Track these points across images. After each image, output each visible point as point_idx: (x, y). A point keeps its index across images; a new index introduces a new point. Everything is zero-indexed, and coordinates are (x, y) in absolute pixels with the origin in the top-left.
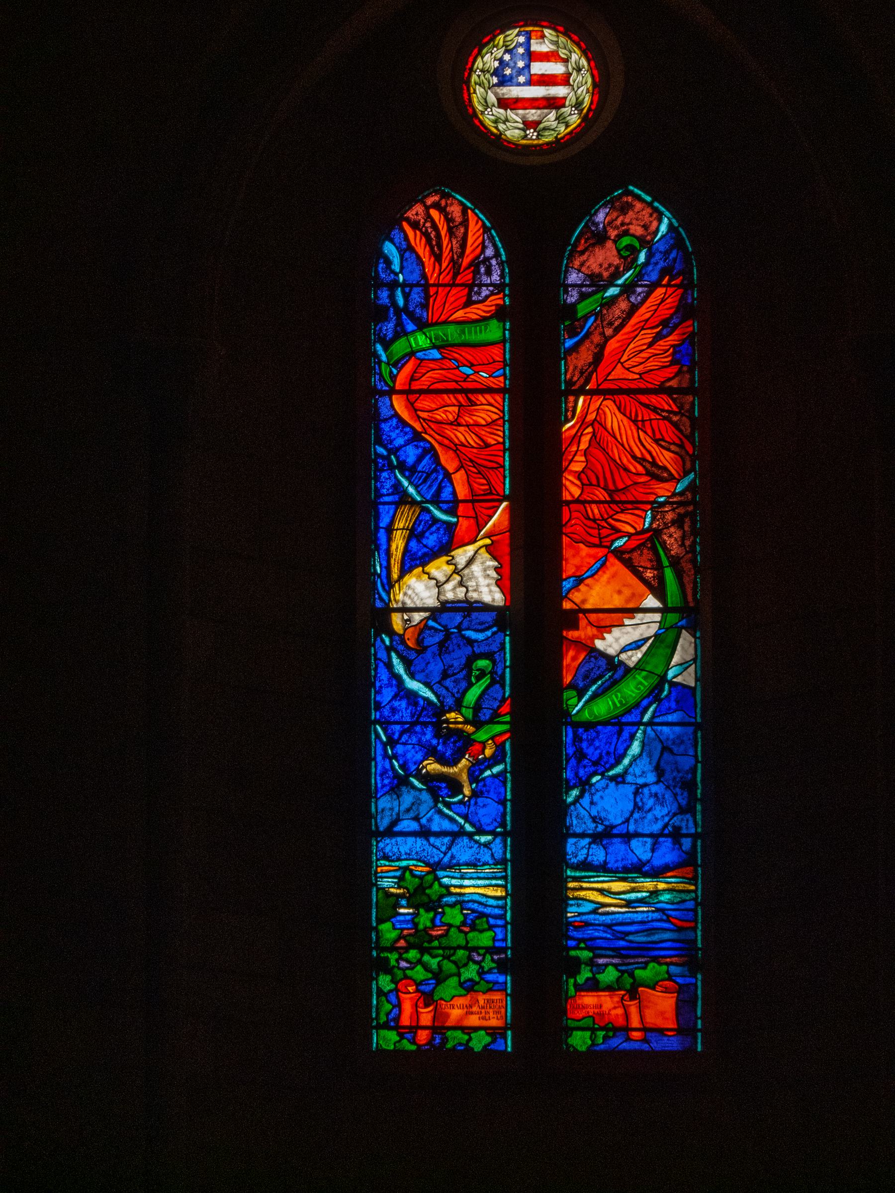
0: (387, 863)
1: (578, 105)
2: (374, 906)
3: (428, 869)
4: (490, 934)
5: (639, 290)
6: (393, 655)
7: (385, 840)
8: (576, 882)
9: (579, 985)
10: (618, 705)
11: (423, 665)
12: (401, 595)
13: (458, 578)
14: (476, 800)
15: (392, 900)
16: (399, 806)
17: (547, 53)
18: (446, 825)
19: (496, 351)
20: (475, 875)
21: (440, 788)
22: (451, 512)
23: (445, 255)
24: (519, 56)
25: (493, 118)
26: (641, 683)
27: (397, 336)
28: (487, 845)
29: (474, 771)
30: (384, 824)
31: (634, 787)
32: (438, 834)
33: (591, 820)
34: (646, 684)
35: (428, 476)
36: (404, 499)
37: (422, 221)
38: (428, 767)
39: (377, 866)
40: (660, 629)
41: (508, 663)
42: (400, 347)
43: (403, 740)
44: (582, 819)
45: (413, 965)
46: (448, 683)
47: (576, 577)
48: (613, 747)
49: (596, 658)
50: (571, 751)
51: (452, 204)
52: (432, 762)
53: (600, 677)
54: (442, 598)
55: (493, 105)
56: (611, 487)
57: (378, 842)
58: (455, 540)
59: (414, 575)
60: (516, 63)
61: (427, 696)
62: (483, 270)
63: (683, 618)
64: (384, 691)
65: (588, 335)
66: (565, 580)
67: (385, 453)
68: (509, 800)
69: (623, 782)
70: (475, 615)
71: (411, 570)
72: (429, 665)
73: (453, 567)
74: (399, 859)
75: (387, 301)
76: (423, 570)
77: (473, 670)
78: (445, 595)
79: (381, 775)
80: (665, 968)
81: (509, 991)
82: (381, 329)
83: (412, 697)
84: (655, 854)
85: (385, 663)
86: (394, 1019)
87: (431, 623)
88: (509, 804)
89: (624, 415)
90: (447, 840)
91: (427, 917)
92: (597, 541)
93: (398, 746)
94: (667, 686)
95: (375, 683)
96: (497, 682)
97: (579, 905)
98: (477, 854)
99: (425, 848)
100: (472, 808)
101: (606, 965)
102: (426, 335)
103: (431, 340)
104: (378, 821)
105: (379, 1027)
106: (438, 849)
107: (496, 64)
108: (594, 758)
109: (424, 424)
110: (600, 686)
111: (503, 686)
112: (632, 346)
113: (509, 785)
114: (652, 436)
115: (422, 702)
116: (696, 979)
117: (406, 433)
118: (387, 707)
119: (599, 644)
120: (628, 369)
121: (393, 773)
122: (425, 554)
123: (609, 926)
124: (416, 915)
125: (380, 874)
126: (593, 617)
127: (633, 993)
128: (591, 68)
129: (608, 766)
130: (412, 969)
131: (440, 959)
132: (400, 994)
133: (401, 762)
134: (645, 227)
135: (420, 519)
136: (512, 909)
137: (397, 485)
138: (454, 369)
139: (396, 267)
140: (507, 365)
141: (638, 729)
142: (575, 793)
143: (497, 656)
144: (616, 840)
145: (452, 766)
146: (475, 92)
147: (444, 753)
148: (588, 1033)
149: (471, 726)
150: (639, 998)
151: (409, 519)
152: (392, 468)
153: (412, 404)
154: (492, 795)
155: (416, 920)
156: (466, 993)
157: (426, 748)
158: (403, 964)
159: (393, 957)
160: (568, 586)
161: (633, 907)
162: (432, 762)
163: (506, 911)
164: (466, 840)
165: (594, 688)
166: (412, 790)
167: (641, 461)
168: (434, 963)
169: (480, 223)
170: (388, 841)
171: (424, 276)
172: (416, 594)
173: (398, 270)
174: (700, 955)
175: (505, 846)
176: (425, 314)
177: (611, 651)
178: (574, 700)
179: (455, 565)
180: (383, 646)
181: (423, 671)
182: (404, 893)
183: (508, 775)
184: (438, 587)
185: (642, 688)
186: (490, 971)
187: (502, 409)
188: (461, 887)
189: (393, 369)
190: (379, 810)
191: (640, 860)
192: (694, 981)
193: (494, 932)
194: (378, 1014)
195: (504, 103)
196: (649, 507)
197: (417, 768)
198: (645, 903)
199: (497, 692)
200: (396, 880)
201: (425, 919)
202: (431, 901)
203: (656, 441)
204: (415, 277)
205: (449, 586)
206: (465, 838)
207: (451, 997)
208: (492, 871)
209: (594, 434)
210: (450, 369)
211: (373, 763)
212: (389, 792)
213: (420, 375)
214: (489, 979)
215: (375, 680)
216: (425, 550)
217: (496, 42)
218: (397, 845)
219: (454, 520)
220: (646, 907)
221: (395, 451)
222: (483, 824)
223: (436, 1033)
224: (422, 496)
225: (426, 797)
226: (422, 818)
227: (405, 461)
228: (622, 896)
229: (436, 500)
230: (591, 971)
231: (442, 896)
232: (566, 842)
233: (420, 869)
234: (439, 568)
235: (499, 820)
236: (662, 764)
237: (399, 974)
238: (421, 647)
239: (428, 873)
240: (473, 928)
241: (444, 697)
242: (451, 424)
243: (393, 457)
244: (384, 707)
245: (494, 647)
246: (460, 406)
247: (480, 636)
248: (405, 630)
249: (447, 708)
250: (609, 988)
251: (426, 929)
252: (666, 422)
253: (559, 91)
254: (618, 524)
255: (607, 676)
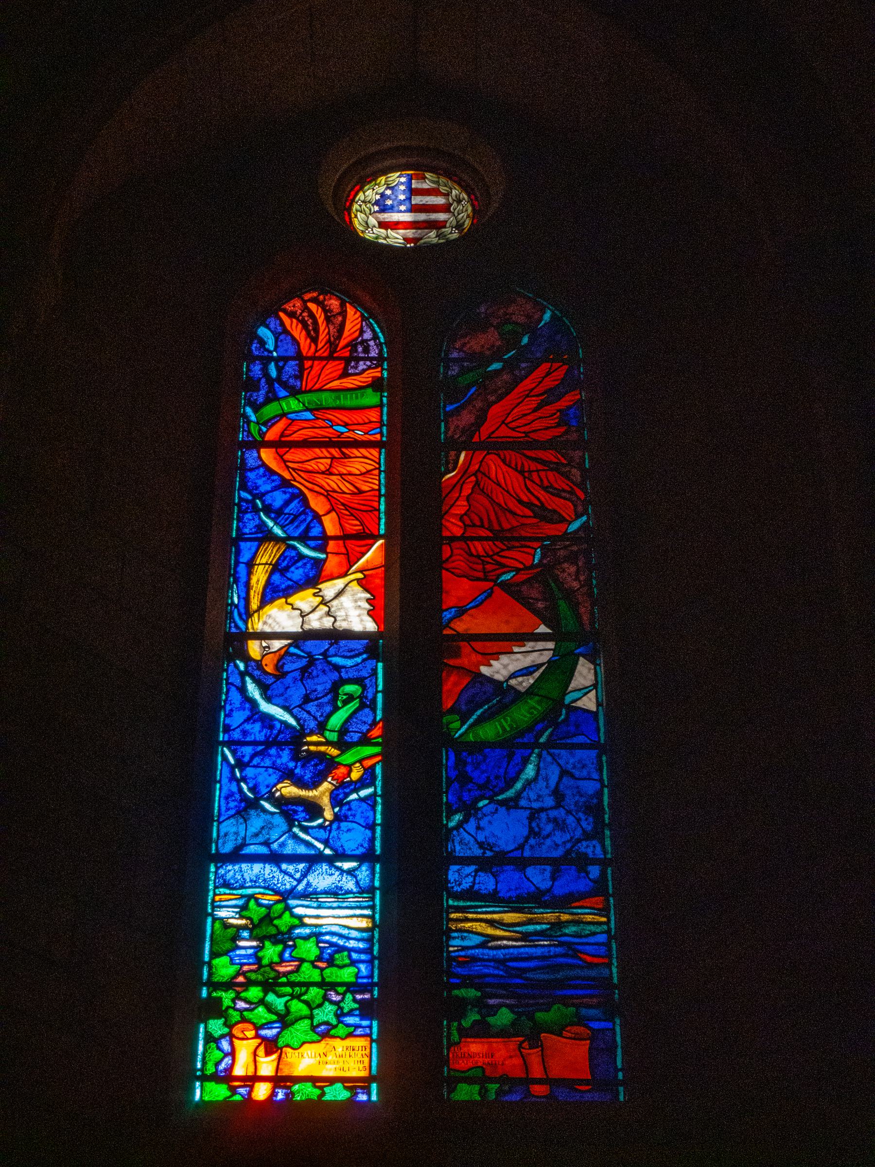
0: (228, 891)
1: (459, 226)
2: (208, 939)
3: (277, 898)
4: (353, 970)
5: (524, 365)
6: (248, 679)
7: (227, 866)
8: (459, 912)
9: (466, 1029)
10: (508, 729)
11: (282, 690)
12: (261, 623)
13: (326, 609)
14: (339, 824)
15: (231, 931)
16: (246, 830)
17: (428, 189)
18: (302, 850)
19: (373, 416)
20: (335, 905)
21: (296, 812)
22: (322, 549)
23: (321, 338)
24: (400, 192)
25: (374, 235)
26: (534, 708)
27: (268, 401)
28: (351, 872)
29: (338, 795)
30: (227, 848)
31: (528, 812)
32: (294, 858)
33: (477, 846)
34: (540, 708)
35: (296, 517)
36: (269, 537)
37: (299, 311)
38: (283, 790)
39: (215, 895)
40: (554, 655)
41: (380, 688)
42: (271, 410)
43: (255, 762)
44: (466, 845)
45: (253, 1005)
46: (312, 707)
47: (458, 607)
48: (502, 771)
49: (481, 683)
50: (453, 774)
51: (330, 299)
52: (287, 785)
53: (487, 701)
54: (306, 627)
55: (374, 226)
56: (496, 527)
57: (217, 868)
58: (324, 574)
59: (276, 606)
60: (397, 197)
61: (284, 719)
62: (360, 349)
63: (579, 647)
64: (235, 714)
65: (470, 401)
66: (446, 610)
67: (249, 497)
68: (379, 825)
69: (517, 807)
70: (343, 643)
71: (272, 601)
72: (288, 690)
73: (321, 599)
74: (242, 887)
75: (259, 373)
76: (286, 602)
77: (339, 694)
78: (310, 625)
79: (227, 798)
80: (572, 1009)
81: (375, 1037)
82: (251, 396)
83: (267, 721)
84: (556, 883)
85: (237, 688)
86: (225, 1070)
87: (293, 650)
88: (378, 830)
89: (509, 466)
90: (301, 866)
91: (274, 951)
92: (481, 575)
93: (248, 769)
94: (564, 711)
95: (224, 707)
96: (367, 706)
97: (463, 938)
98: (339, 881)
99: (275, 875)
100: (334, 833)
101: (500, 1006)
102: (299, 401)
103: (304, 405)
104: (220, 845)
105: (204, 1078)
106: (291, 876)
107: (378, 197)
108: (482, 782)
109: (293, 473)
110: (486, 711)
111: (374, 710)
112: (515, 411)
113: (379, 808)
114: (539, 484)
115: (278, 726)
116: (614, 1023)
117: (273, 481)
118: (238, 730)
119: (484, 670)
120: (513, 429)
121: (240, 796)
122: (288, 587)
123: (500, 962)
124: (260, 948)
125: (218, 903)
126: (478, 645)
127: (534, 1039)
128: (471, 200)
129: (497, 790)
130: (252, 1010)
131: (288, 998)
132: (234, 1040)
133: (251, 785)
134: (528, 317)
135: (286, 555)
136: (379, 941)
137: (264, 524)
138: (326, 427)
139: (271, 345)
140: (384, 425)
141: (532, 752)
142: (458, 817)
143: (367, 681)
144: (508, 867)
145: (312, 789)
146: (356, 216)
147: (302, 777)
148: (477, 1088)
149: (335, 748)
150: (542, 1046)
151: (273, 555)
152: (256, 511)
153: (281, 457)
154: (358, 819)
155: (260, 954)
156: (319, 1038)
157: (281, 771)
158: (241, 1005)
159: (227, 997)
160: (449, 616)
161: (530, 941)
162: (287, 785)
163: (373, 945)
164: (325, 866)
165: (479, 712)
166: (262, 814)
167: (529, 505)
168: (279, 1003)
169: (358, 313)
170: (230, 867)
171: (299, 351)
172: (278, 623)
173: (272, 349)
174: (617, 996)
175: (373, 873)
176: (299, 383)
177: (499, 677)
178: (457, 724)
179: (322, 596)
180: (237, 672)
181: (282, 695)
182: (246, 925)
183: (379, 799)
184: (303, 617)
185: (535, 713)
186: (350, 1013)
187: (377, 461)
188: (318, 917)
189: (262, 427)
190: (222, 834)
191: (538, 888)
192: (609, 1025)
193: (357, 967)
194: (204, 1063)
195: (383, 225)
196: (539, 544)
197: (270, 791)
198: (547, 936)
199: (366, 716)
200: (238, 910)
201: (271, 952)
202: (280, 932)
203: (545, 489)
204: (291, 352)
205: (313, 617)
206: (324, 864)
207: (300, 1044)
208: (356, 899)
209: (477, 483)
210: (322, 427)
211: (218, 786)
212: (235, 814)
213: (291, 432)
214: (348, 1022)
215: (225, 704)
216: (290, 583)
217: (378, 182)
218: (241, 871)
219: (323, 556)
220: (546, 941)
221: (261, 496)
222: (346, 849)
223: (281, 1087)
224: (286, 534)
225: (279, 820)
226: (273, 843)
227: (271, 505)
228: (518, 929)
229: (304, 538)
230: (479, 1013)
231: (293, 927)
232: (448, 870)
233: (268, 897)
234: (304, 599)
235: (366, 845)
236: (561, 787)
237: (235, 1016)
238: (279, 671)
239: (278, 902)
240: (331, 963)
241: (305, 721)
242: (323, 473)
243: (258, 501)
244: (234, 730)
245: (364, 673)
246: (333, 458)
247: (349, 663)
248: (263, 656)
249: (308, 731)
250: (503, 1033)
251: (271, 965)
252: (554, 472)
253: (442, 216)
254: (503, 561)
255: (495, 701)
